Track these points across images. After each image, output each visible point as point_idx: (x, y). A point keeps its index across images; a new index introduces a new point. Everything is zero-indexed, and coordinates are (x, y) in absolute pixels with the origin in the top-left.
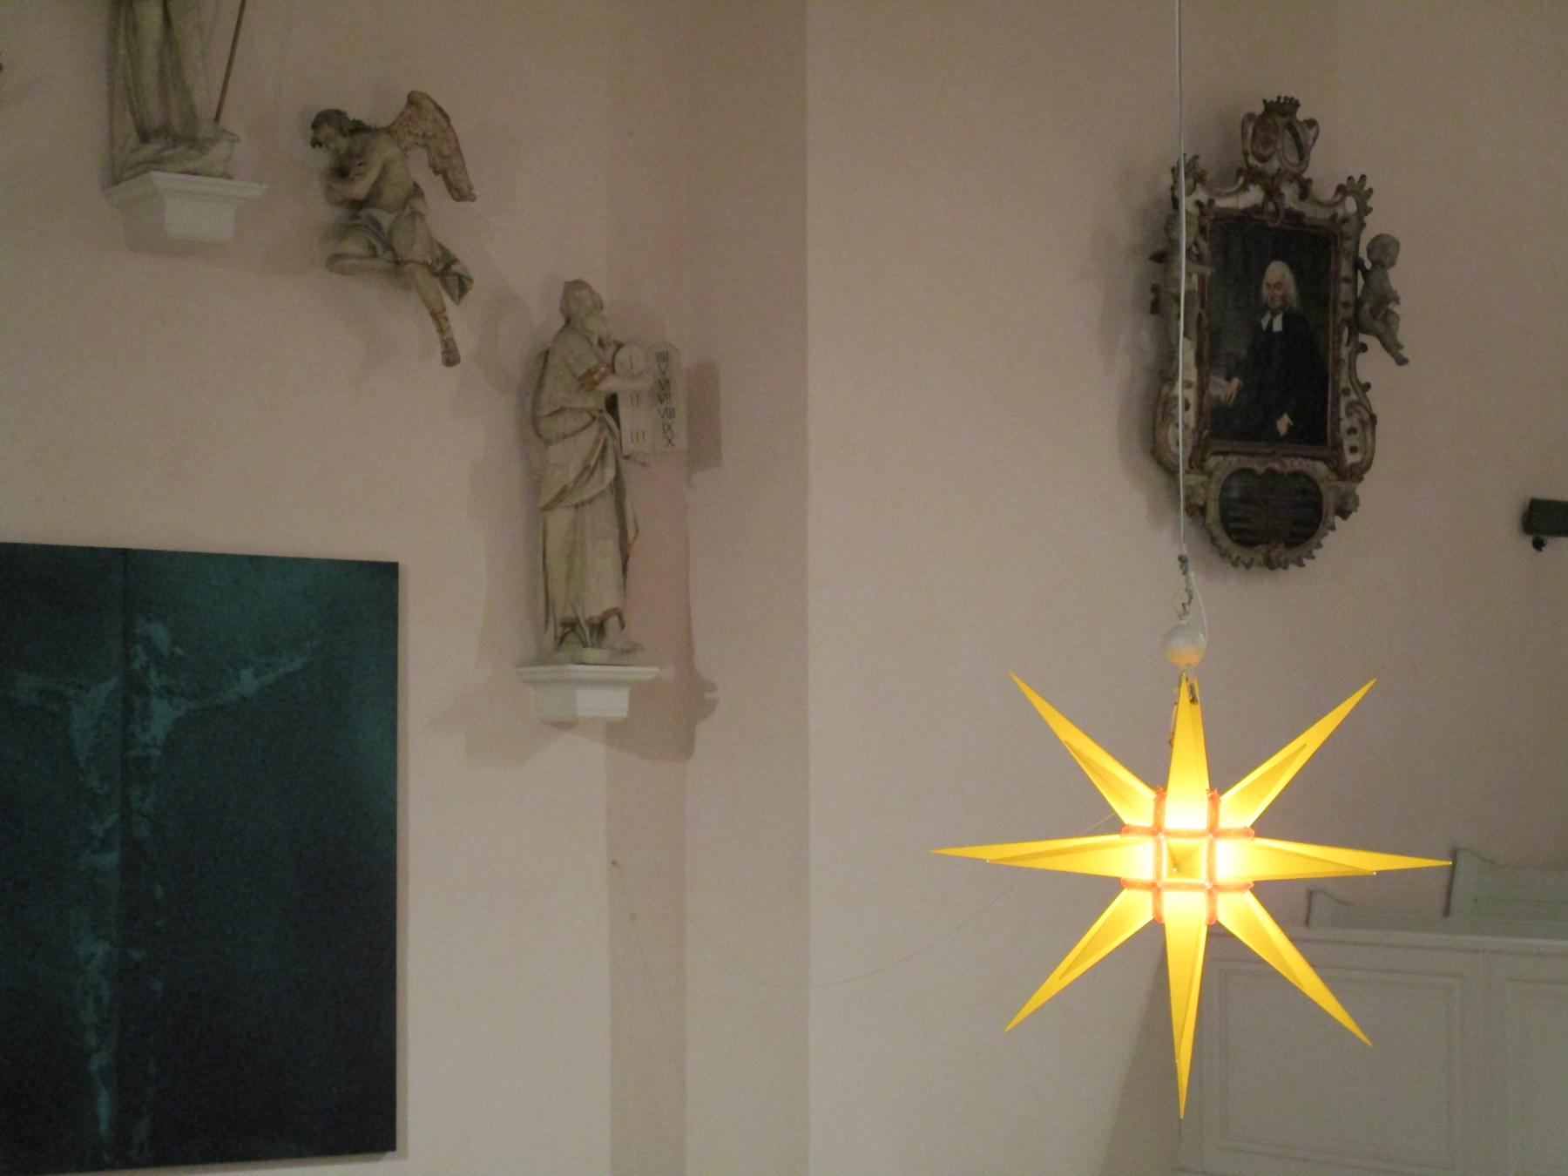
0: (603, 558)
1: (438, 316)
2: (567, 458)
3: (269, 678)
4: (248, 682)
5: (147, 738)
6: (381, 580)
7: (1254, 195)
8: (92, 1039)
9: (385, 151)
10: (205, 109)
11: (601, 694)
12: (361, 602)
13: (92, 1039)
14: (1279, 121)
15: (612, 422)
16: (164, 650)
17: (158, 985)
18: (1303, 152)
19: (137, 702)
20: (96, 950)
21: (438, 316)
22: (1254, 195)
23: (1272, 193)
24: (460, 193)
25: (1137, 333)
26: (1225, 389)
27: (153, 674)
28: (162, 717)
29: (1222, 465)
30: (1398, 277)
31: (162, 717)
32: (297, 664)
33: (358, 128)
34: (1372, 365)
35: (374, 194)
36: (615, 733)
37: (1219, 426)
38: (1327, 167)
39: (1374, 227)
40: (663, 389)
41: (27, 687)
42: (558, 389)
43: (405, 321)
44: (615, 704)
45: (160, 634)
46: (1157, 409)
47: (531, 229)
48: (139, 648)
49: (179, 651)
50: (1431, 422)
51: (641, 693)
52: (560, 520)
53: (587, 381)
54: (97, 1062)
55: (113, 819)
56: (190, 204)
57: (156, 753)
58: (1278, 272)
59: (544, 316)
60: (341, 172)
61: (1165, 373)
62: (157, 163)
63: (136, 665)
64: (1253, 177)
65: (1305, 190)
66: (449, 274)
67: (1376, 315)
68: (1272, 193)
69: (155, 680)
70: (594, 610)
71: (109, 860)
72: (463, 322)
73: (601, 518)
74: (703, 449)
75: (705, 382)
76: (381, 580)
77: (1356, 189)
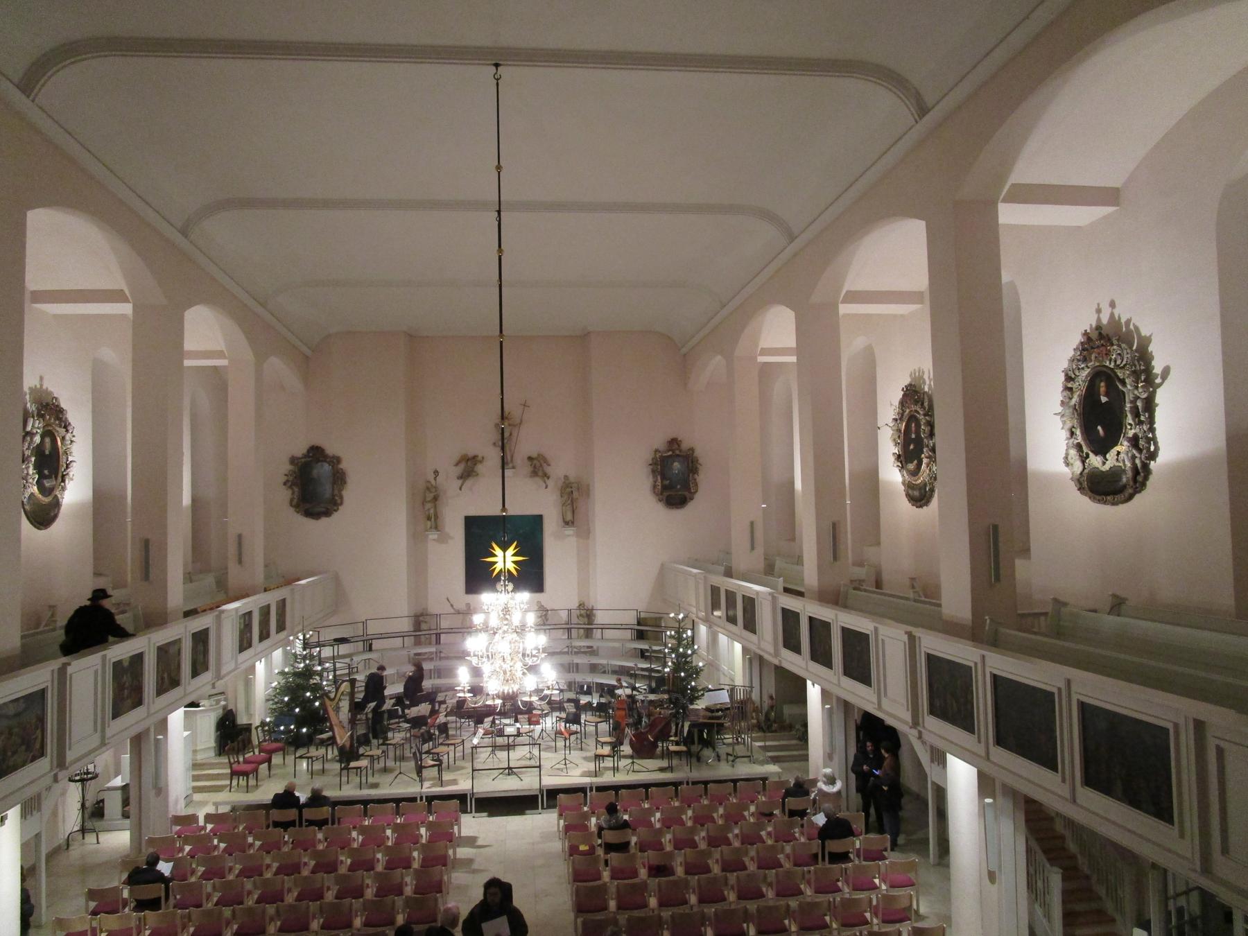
6: (540, 517)
12: (538, 520)
29: (665, 494)
35: (538, 467)
37: (664, 488)
38: (685, 446)
46: (654, 487)
58: (676, 465)
66: (546, 476)
72: (550, 483)
73: (569, 507)
74: (588, 495)
76: (540, 517)
77: (692, 450)
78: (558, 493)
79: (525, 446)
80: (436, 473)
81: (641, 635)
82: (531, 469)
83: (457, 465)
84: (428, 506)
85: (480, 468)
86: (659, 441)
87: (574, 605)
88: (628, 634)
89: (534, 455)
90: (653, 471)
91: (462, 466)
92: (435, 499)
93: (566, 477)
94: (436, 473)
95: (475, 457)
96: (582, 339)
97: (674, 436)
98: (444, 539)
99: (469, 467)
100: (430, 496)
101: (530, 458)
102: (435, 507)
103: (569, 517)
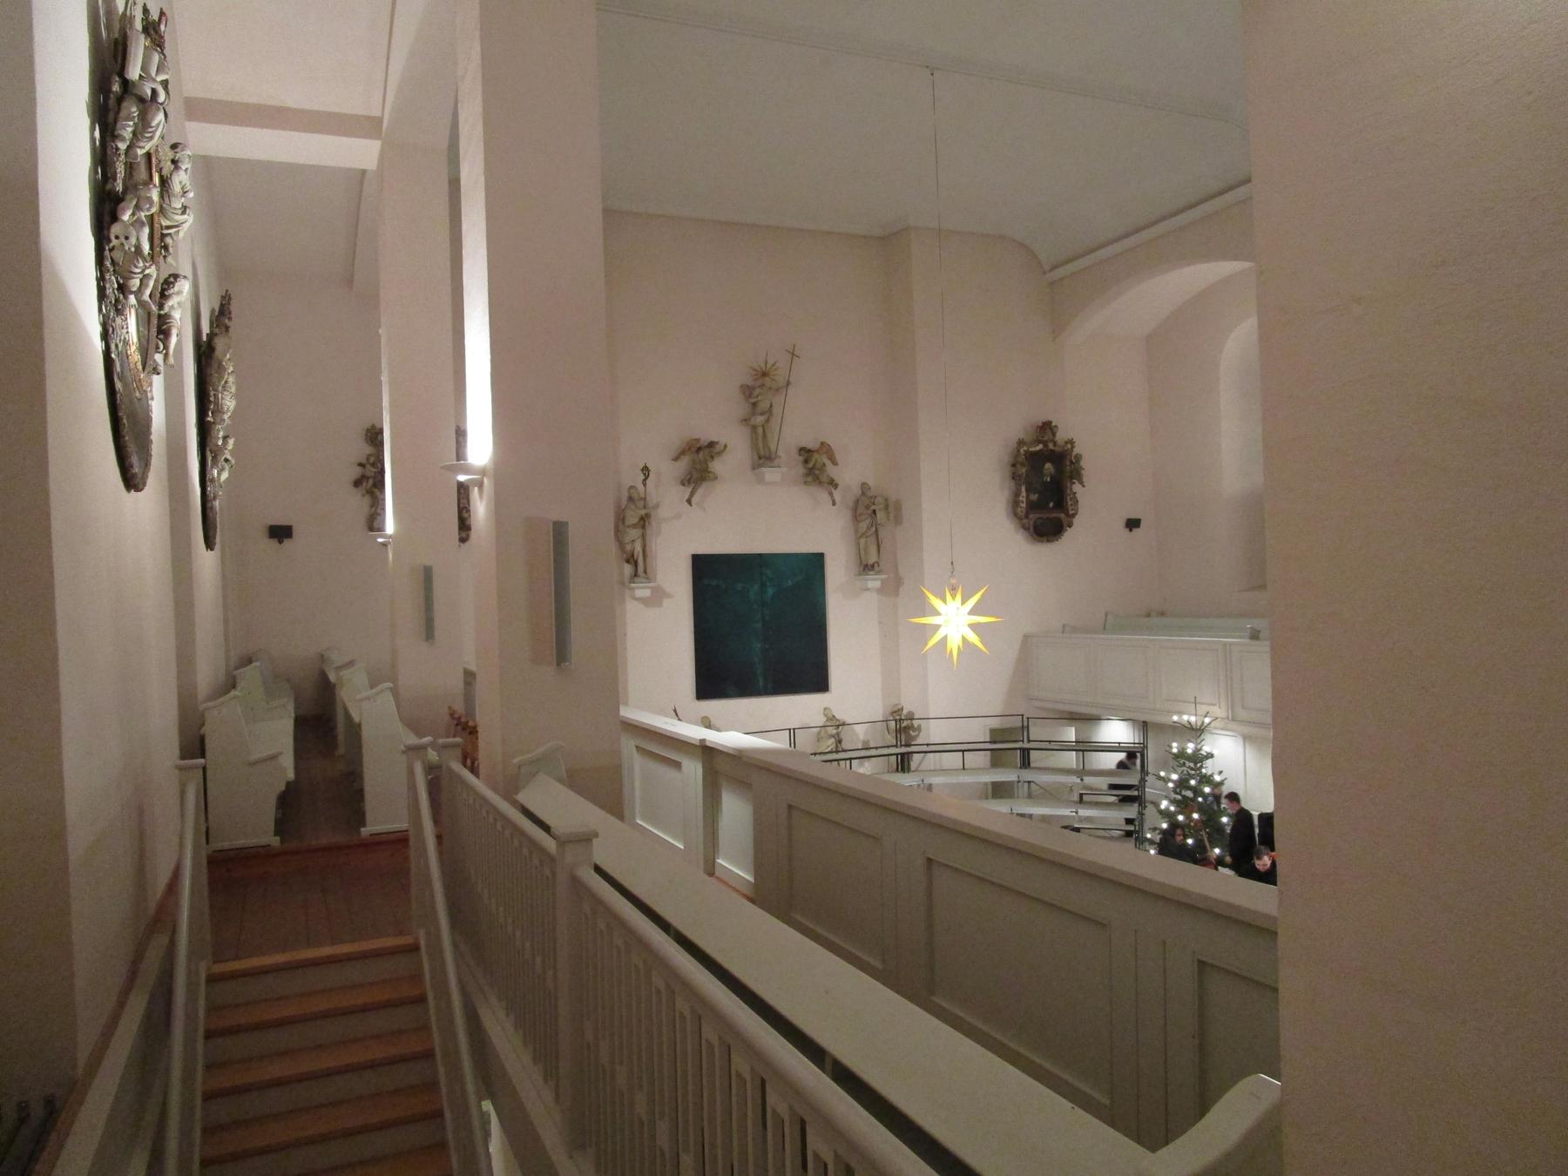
0: (873, 549)
1: (831, 494)
2: (863, 526)
4: (790, 583)
7: (1040, 446)
9: (816, 456)
10: (773, 448)
11: (874, 582)
12: (815, 563)
14: (1047, 428)
15: (875, 517)
18: (1054, 434)
20: (757, 646)
21: (831, 494)
22: (1040, 446)
23: (1046, 445)
24: (835, 463)
25: (1010, 484)
26: (1034, 497)
28: (770, 591)
30: (1082, 463)
31: (770, 591)
33: (809, 451)
34: (1077, 487)
35: (815, 466)
36: (880, 591)
37: (1032, 507)
38: (1061, 436)
39: (1076, 451)
40: (887, 507)
41: (739, 586)
42: (861, 509)
43: (823, 495)
44: (877, 584)
45: (769, 572)
46: (1015, 503)
47: (852, 471)
50: (1096, 503)
51: (883, 582)
52: (863, 541)
53: (867, 507)
56: (770, 474)
58: (1048, 466)
59: (858, 492)
60: (806, 461)
61: (1017, 494)
62: (760, 466)
64: (1040, 442)
65: (1055, 444)
66: (833, 484)
67: (1077, 475)
68: (1046, 445)
70: (871, 562)
71: (759, 625)
72: (837, 495)
73: (873, 539)
74: (898, 520)
75: (898, 507)
77: (1071, 442)
78: (848, 514)
79: (794, 430)
80: (645, 470)
81: (997, 760)
82: (801, 470)
83: (676, 459)
84: (634, 533)
85: (717, 466)
86: (1014, 425)
87: (877, 711)
88: (982, 759)
89: (810, 446)
90: (1014, 477)
91: (684, 463)
92: (644, 521)
93: (864, 487)
94: (645, 470)
95: (712, 444)
96: (889, 245)
97: (1041, 418)
98: (658, 597)
99: (698, 463)
100: (632, 517)
101: (802, 450)
102: (643, 537)
103: (872, 559)
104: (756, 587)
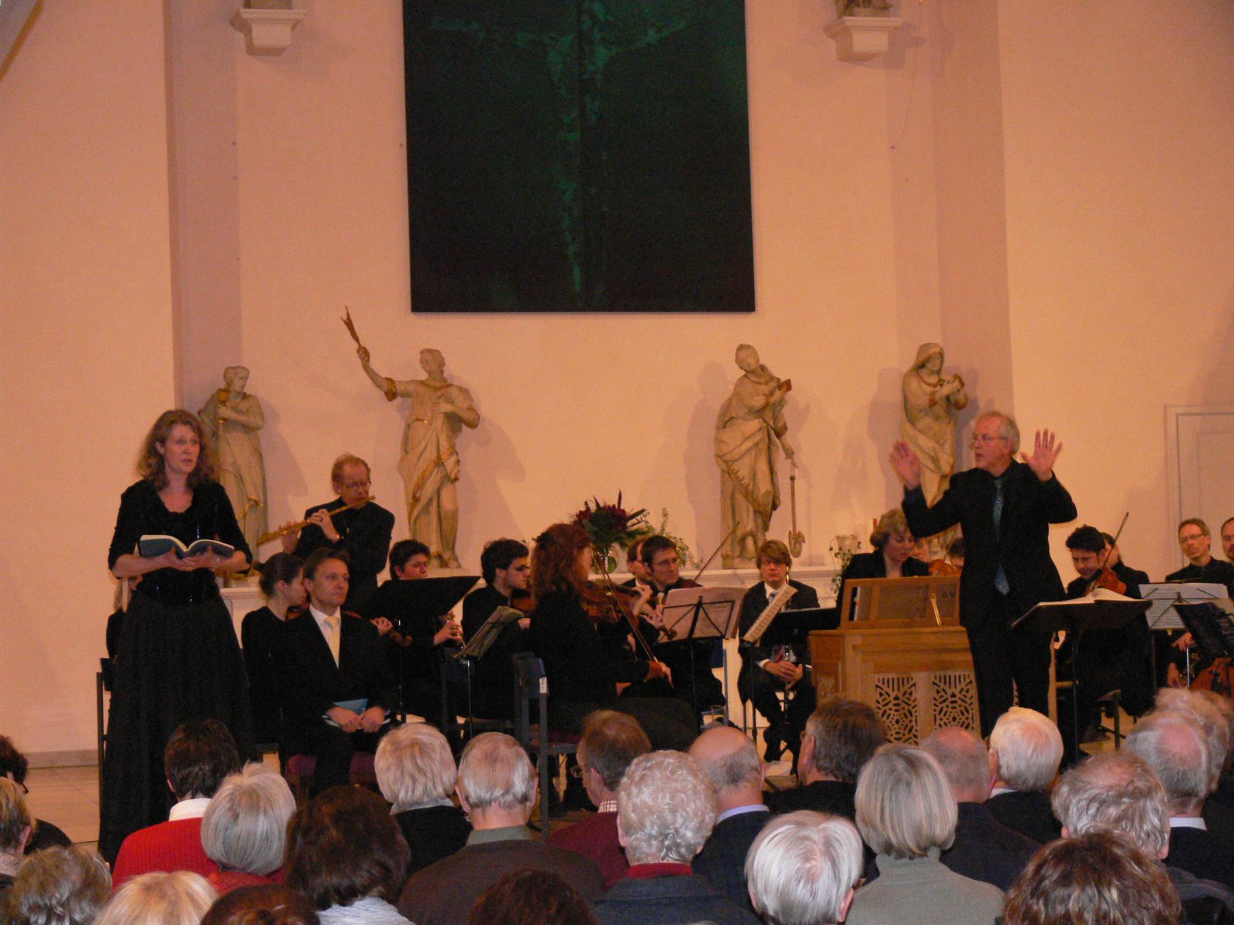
3: (666, 32)
5: (592, 68)
8: (568, 238)
13: (568, 238)
16: (601, 17)
17: (605, 209)
19: (586, 48)
27: (596, 30)
28: (601, 55)
31: (601, 55)
32: (683, 25)
48: (586, 18)
49: (610, 18)
54: (571, 250)
55: (575, 114)
57: (599, 76)
63: (585, 27)
69: (597, 35)
71: (574, 136)
104: (567, 39)
